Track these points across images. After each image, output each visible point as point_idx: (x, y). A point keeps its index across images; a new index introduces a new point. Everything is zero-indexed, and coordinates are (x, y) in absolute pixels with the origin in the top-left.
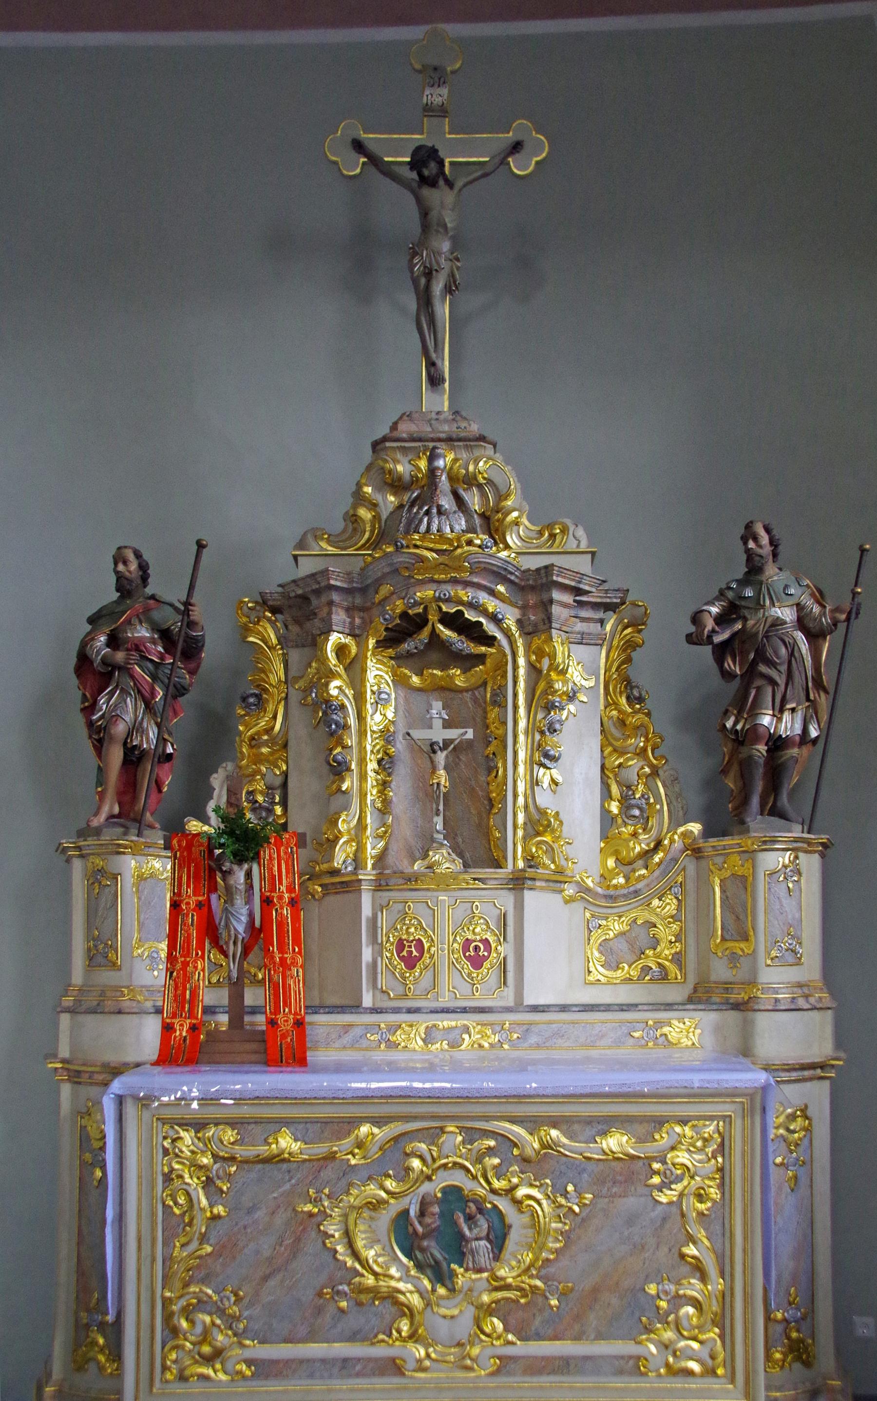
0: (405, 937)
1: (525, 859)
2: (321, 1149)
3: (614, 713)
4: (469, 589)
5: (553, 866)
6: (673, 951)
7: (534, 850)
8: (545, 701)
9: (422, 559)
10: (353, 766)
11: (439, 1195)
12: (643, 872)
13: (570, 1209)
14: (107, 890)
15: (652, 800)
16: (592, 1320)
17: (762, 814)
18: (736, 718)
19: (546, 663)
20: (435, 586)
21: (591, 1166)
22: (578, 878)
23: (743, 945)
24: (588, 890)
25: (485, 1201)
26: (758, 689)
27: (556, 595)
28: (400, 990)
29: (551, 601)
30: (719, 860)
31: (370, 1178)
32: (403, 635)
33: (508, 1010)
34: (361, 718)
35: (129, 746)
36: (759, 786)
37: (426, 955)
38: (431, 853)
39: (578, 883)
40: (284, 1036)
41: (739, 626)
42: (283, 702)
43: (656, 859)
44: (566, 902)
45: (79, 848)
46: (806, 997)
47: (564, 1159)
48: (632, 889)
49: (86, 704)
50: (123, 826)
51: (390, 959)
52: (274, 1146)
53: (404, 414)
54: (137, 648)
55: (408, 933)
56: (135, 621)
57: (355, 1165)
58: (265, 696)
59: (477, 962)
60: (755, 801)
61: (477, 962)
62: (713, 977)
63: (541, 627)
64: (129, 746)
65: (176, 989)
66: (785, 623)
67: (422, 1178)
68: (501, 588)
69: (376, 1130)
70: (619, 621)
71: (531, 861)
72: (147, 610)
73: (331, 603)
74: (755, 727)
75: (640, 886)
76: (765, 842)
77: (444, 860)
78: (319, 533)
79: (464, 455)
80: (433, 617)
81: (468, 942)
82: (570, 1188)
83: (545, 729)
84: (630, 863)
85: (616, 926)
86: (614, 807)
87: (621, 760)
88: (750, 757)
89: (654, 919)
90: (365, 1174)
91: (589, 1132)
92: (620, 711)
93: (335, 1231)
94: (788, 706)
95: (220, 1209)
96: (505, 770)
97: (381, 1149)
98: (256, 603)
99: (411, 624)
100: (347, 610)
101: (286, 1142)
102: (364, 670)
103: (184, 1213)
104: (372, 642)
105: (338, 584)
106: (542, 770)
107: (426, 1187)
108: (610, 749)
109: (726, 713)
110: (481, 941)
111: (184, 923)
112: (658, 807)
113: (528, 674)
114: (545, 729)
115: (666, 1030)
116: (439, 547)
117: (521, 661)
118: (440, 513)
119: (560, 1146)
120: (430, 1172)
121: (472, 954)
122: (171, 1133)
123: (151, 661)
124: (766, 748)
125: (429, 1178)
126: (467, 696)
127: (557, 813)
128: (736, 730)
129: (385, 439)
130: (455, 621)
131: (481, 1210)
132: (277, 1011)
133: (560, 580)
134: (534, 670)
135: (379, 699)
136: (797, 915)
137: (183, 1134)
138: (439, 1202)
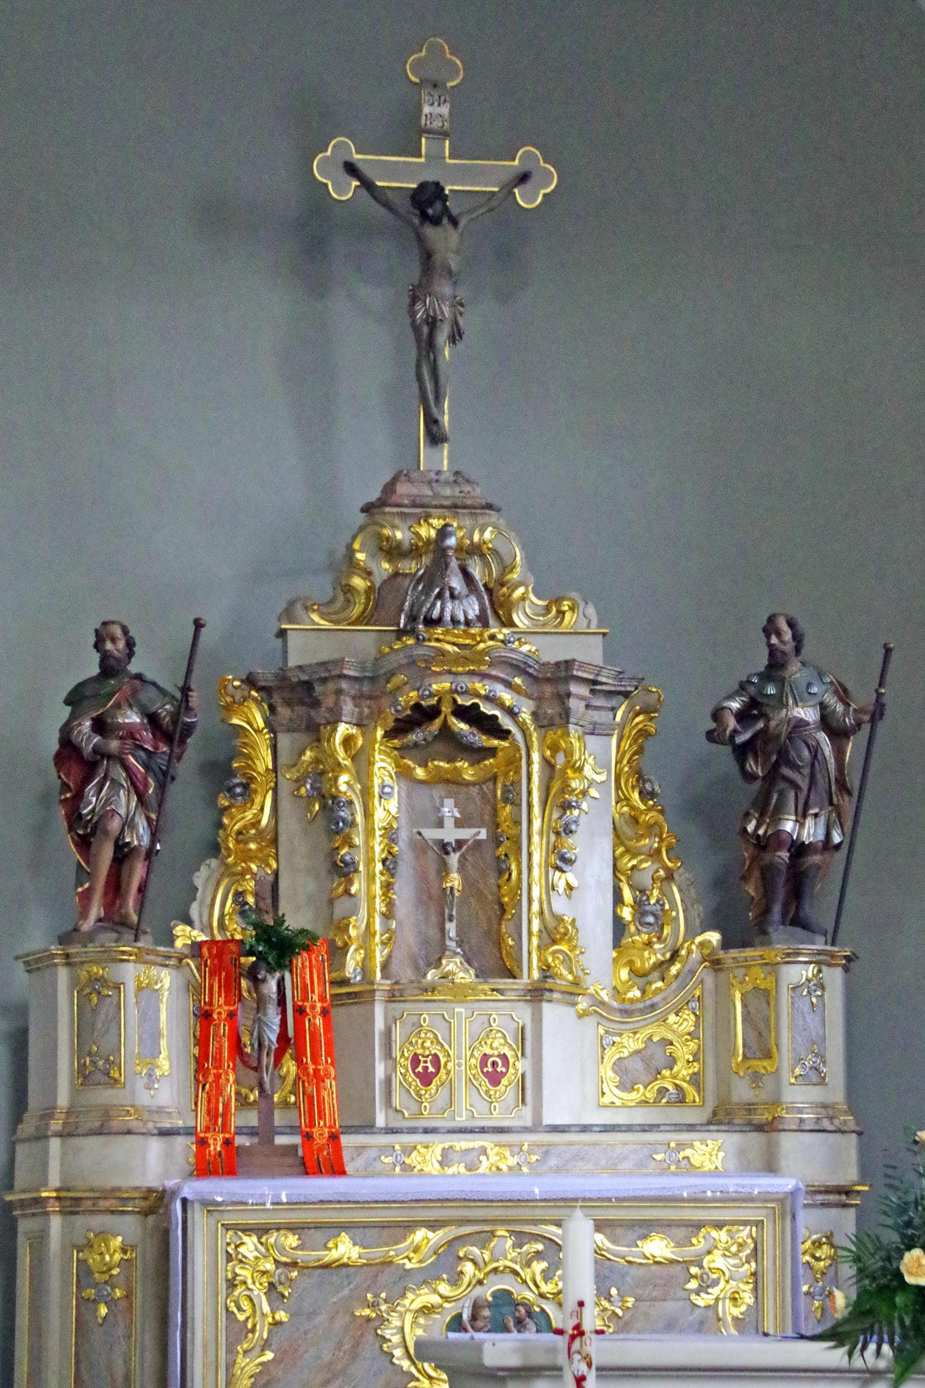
0: (419, 1052)
1: (541, 970)
2: (378, 1253)
3: (626, 809)
4: (486, 682)
5: (570, 977)
6: (691, 1071)
7: (550, 959)
8: (560, 799)
9: (443, 653)
10: (361, 868)
11: (490, 1299)
12: (660, 984)
13: (613, 1312)
14: (108, 1000)
15: (667, 907)
17: (783, 923)
18: (758, 822)
19: (560, 760)
20: (451, 678)
21: (633, 1271)
22: (591, 990)
23: (765, 1063)
24: (602, 1003)
25: (533, 1305)
27: (574, 688)
28: (414, 1107)
29: (569, 695)
30: (741, 972)
31: (425, 1282)
33: (526, 1130)
34: (368, 814)
35: (120, 843)
36: (781, 894)
37: (443, 1071)
38: (444, 962)
39: (592, 996)
40: (320, 1150)
42: (270, 792)
43: (674, 970)
44: (580, 1016)
45: (67, 956)
46: (831, 1118)
47: (608, 1262)
48: (648, 1003)
49: (68, 795)
50: (116, 931)
51: (404, 1076)
52: (334, 1251)
53: (401, 472)
54: (132, 736)
55: (423, 1047)
56: (125, 706)
57: (411, 1269)
58: (253, 786)
59: (495, 1079)
60: (777, 909)
61: (495, 1079)
62: (735, 1098)
63: (557, 720)
64: (120, 843)
65: (209, 1101)
67: (474, 1282)
68: (518, 680)
69: (430, 1235)
70: (630, 708)
71: (547, 972)
72: (134, 693)
73: (339, 692)
74: (778, 833)
75: (657, 999)
76: (788, 955)
78: (309, 604)
79: (468, 522)
80: (446, 709)
81: (485, 1057)
82: (614, 1291)
83: (561, 830)
84: (645, 975)
85: (631, 1044)
86: (627, 913)
87: (634, 862)
89: (670, 1036)
90: (419, 1278)
91: (631, 1235)
92: (632, 808)
93: (392, 1335)
95: (282, 1316)
96: (520, 873)
97: (435, 1253)
98: (242, 681)
99: (423, 714)
100: (354, 698)
101: (345, 1249)
102: (371, 763)
103: (248, 1319)
104: (380, 733)
105: (351, 673)
106: (558, 874)
107: (478, 1291)
108: (621, 849)
109: (747, 816)
110: (499, 1056)
111: (216, 1034)
112: (674, 914)
113: (542, 770)
114: (561, 830)
115: (688, 1152)
116: (461, 641)
117: (536, 757)
118: (453, 597)
119: (603, 1250)
120: (482, 1276)
121: (490, 1069)
122: (235, 1239)
123: (146, 750)
124: (788, 854)
125: (480, 1282)
126: (474, 791)
127: (574, 920)
128: (758, 835)
129: (382, 502)
130: (470, 714)
131: (530, 1314)
132: (311, 1124)
133: (580, 674)
134: (548, 764)
135: (384, 796)
136: (821, 1033)
137: (246, 1239)
138: (490, 1306)
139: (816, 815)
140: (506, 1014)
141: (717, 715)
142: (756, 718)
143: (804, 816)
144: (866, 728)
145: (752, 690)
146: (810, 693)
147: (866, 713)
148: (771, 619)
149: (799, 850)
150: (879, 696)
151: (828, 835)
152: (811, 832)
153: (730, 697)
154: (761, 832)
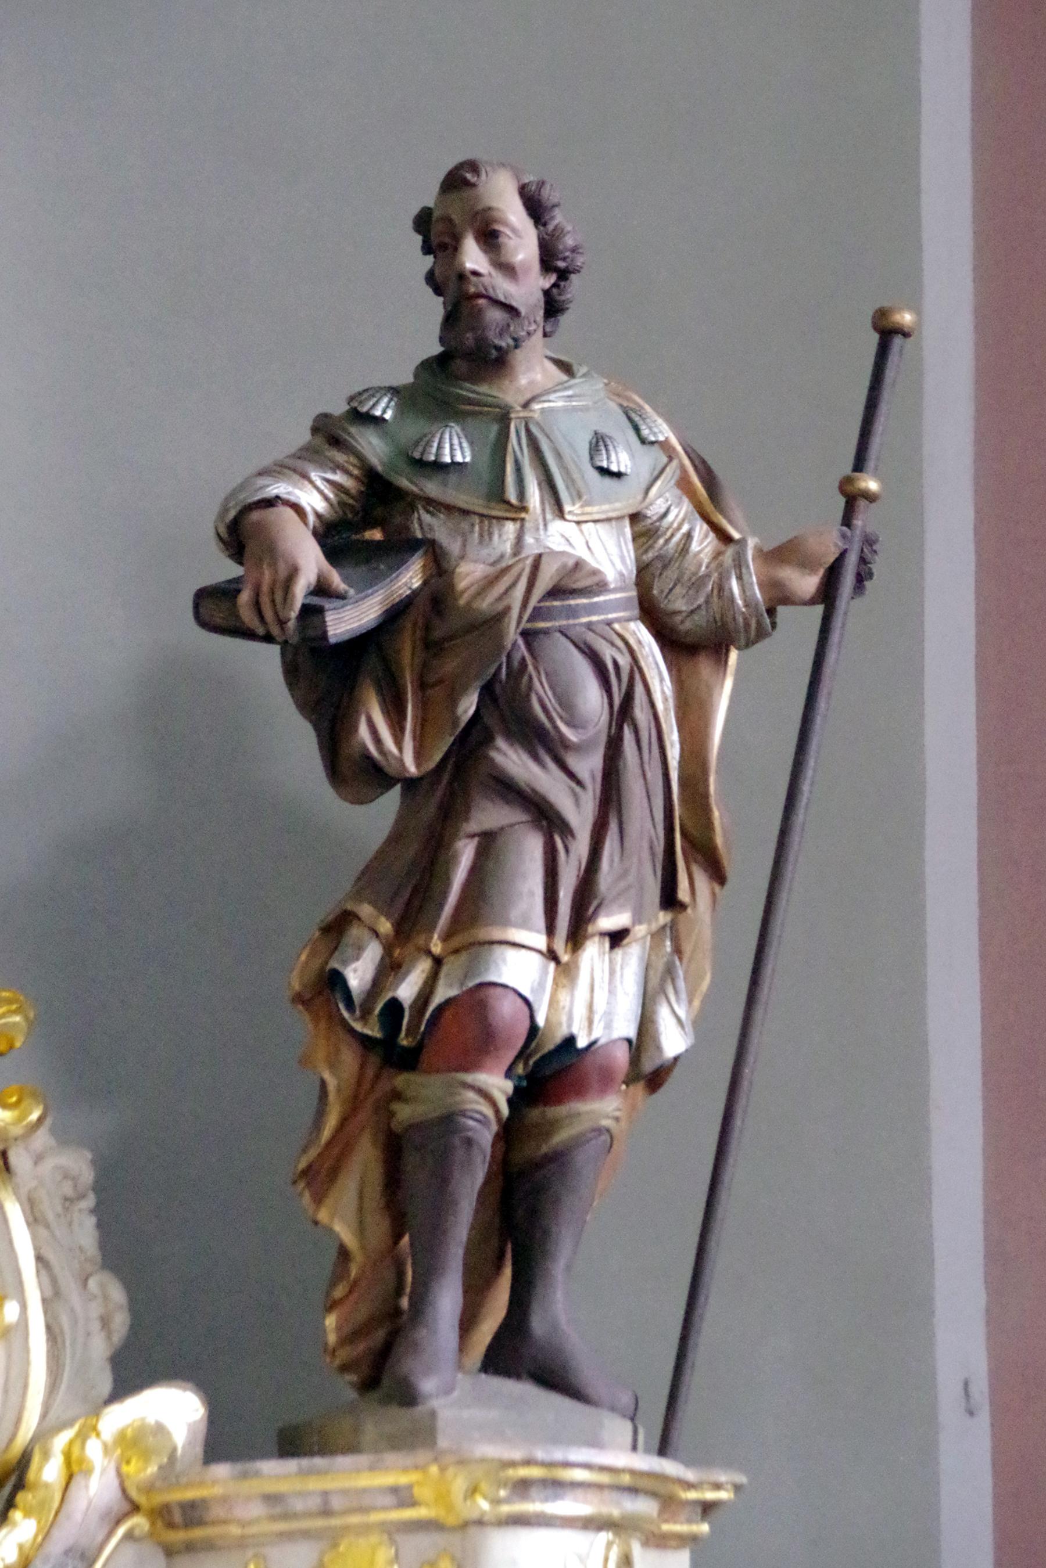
18: (388, 949)
26: (488, 841)
41: (411, 577)
66: (602, 587)
74: (478, 999)
76: (523, 1487)
88: (448, 1123)
94: (608, 922)
124: (509, 1086)
128: (394, 1007)
139: (617, 938)
141: (243, 532)
142: (401, 547)
143: (576, 938)
144: (800, 624)
145: (373, 447)
146: (605, 472)
147: (806, 564)
148: (458, 180)
149: (552, 1071)
150: (853, 499)
151: (646, 1023)
152: (597, 999)
153: (290, 468)
154: (407, 991)
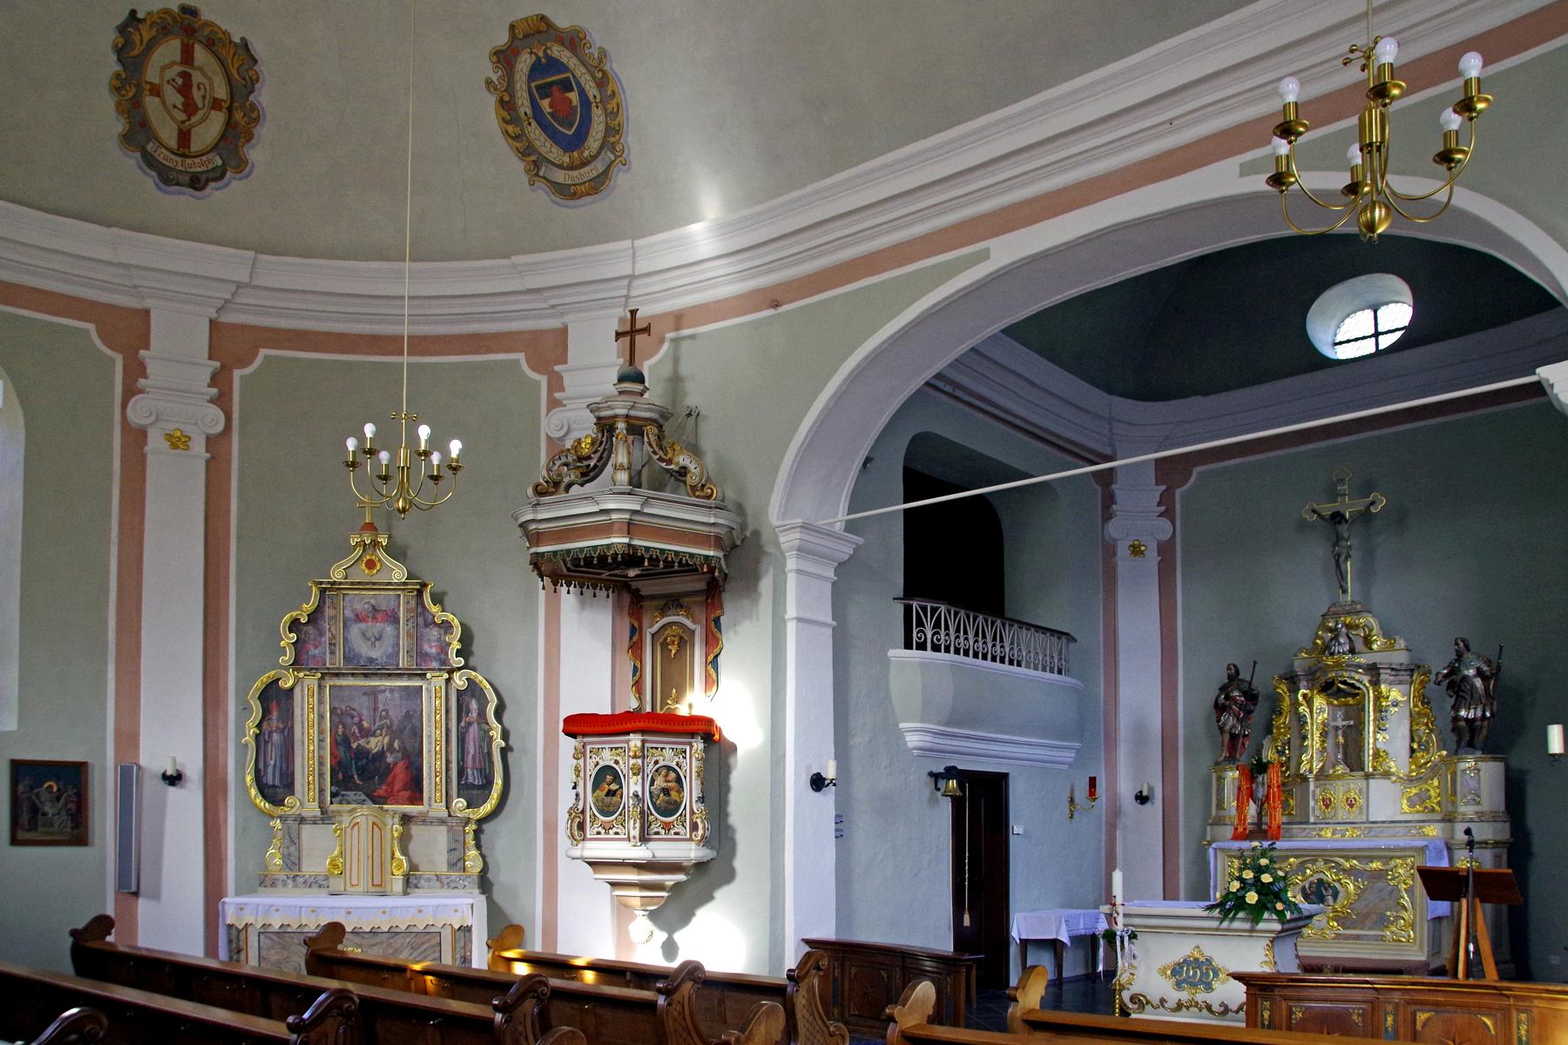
16: (1368, 923)
32: (1328, 688)
59: (1351, 806)
61: (1351, 806)
77: (1341, 769)
130: (1344, 683)
135: (1320, 710)
140: (1355, 784)
